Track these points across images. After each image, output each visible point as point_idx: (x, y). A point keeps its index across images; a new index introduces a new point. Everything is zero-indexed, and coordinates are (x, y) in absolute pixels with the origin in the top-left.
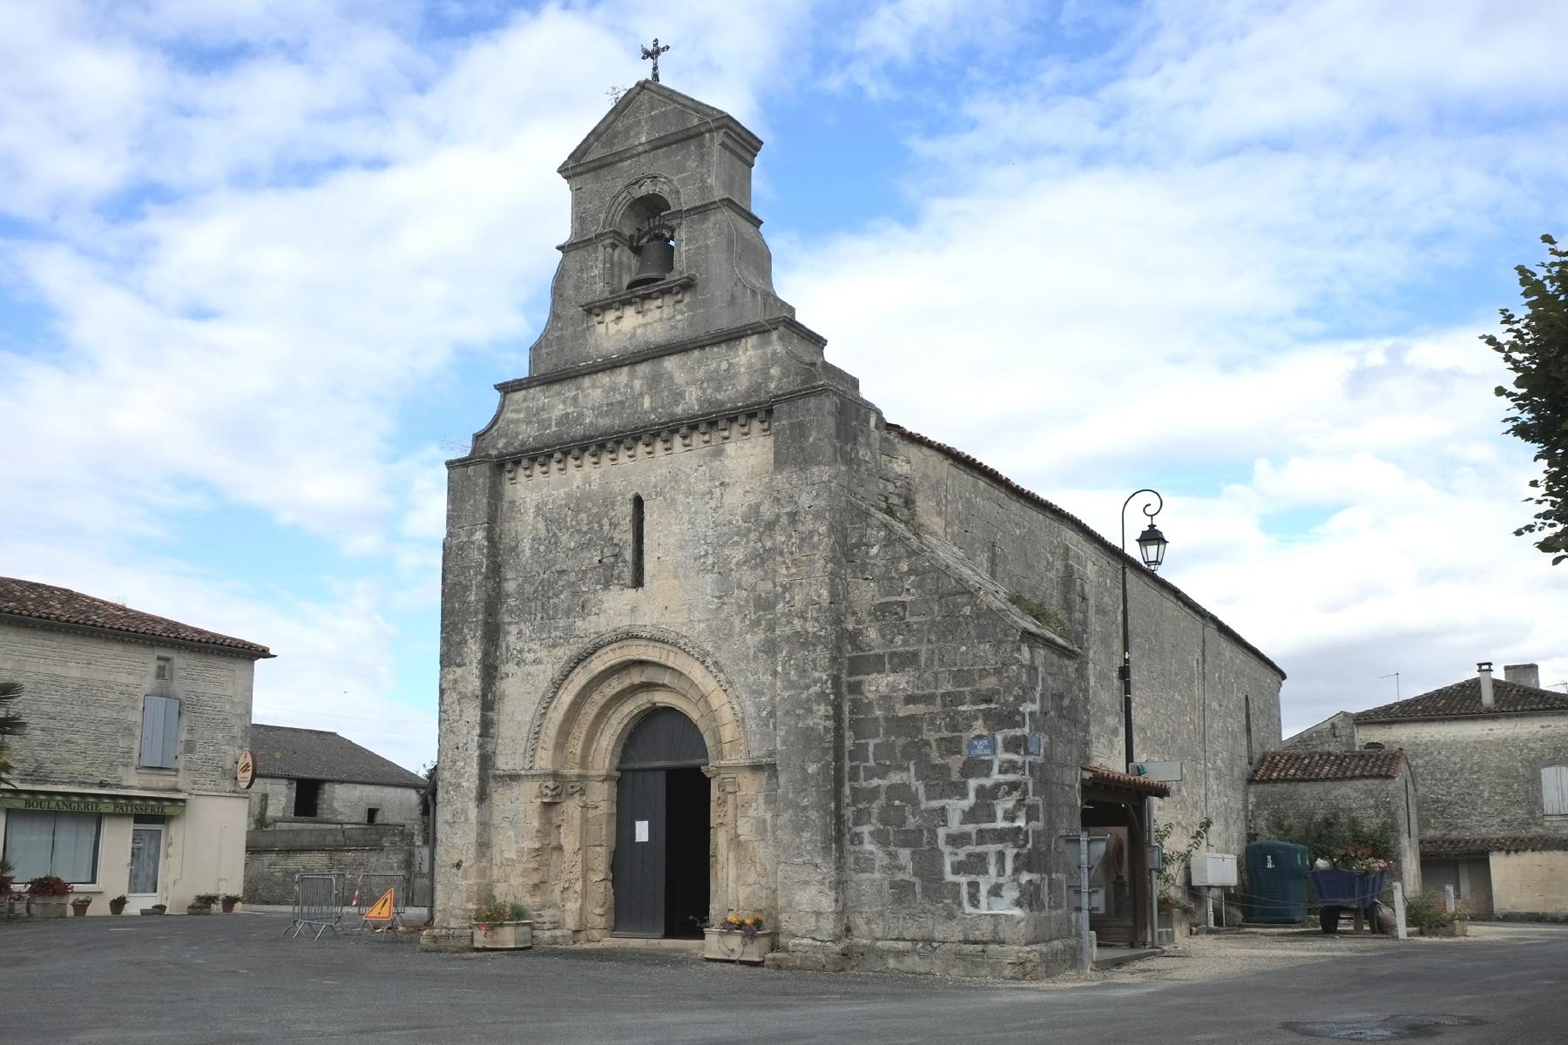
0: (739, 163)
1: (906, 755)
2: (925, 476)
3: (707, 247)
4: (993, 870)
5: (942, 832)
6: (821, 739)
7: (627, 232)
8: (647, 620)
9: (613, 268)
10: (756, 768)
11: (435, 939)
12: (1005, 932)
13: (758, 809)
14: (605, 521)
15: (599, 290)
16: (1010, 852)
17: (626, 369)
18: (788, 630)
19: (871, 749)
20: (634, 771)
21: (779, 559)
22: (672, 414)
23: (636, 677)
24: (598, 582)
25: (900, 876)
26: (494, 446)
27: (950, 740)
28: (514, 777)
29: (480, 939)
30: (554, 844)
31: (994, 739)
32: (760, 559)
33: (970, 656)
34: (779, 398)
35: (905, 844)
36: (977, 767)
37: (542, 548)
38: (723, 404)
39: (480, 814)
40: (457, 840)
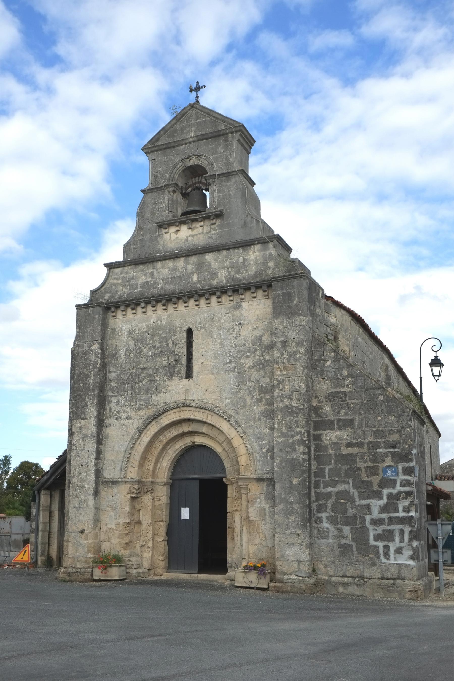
0: (244, 151)
1: (347, 475)
2: (342, 325)
3: (230, 195)
4: (397, 539)
5: (368, 518)
6: (301, 465)
7: (180, 184)
8: (195, 397)
9: (173, 204)
10: (260, 480)
11: (69, 574)
12: (405, 573)
13: (262, 503)
14: (170, 341)
15: (166, 215)
16: (407, 530)
17: (183, 259)
18: (281, 405)
19: (327, 471)
20: (180, 480)
21: (276, 366)
22: (210, 285)
23: (186, 428)
24: (166, 375)
25: (343, 541)
26: (103, 298)
27: (373, 467)
28: (114, 482)
29: (98, 573)
30: (137, 520)
31: (398, 468)
32: (261, 366)
33: (383, 422)
34: (276, 279)
35: (346, 524)
36: (387, 483)
37: (132, 355)
38: (240, 280)
39: (95, 503)
40: (81, 517)
